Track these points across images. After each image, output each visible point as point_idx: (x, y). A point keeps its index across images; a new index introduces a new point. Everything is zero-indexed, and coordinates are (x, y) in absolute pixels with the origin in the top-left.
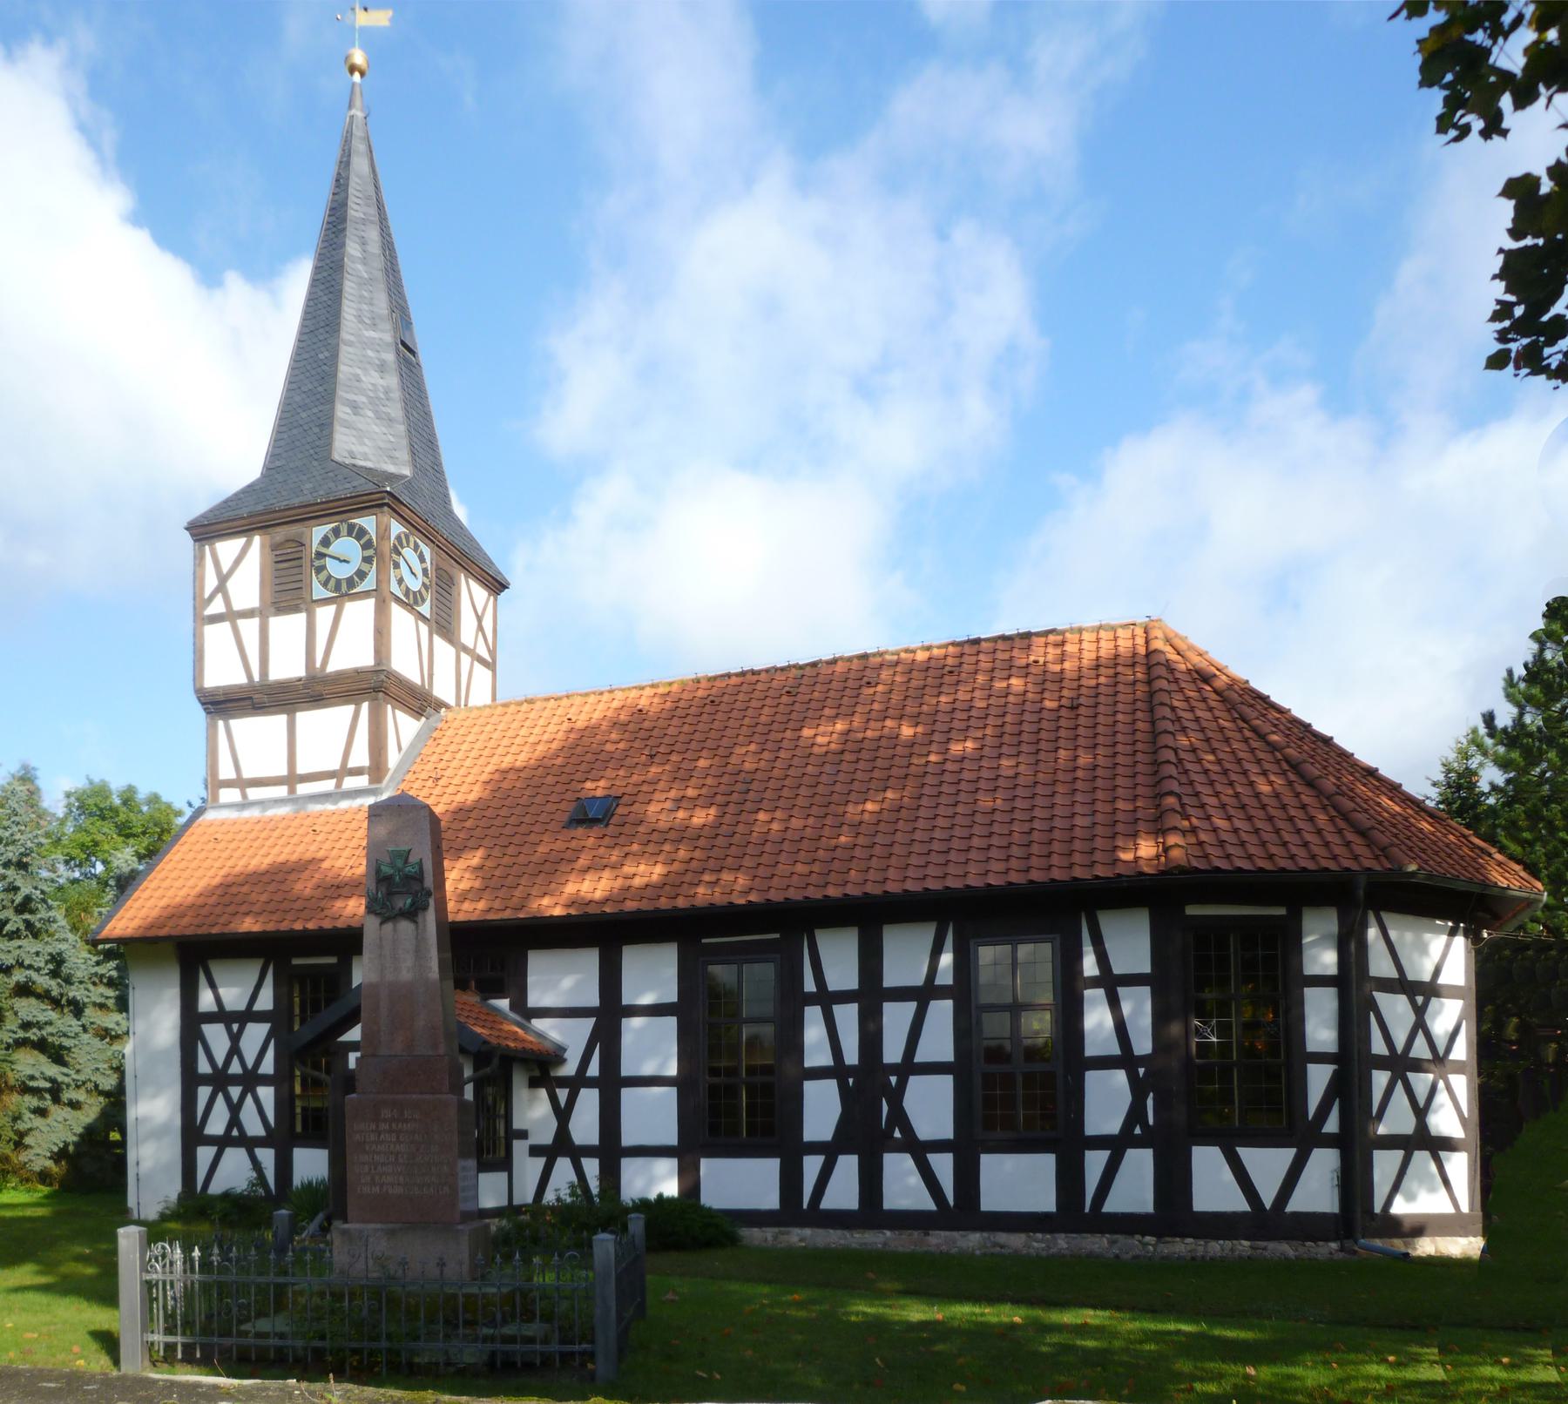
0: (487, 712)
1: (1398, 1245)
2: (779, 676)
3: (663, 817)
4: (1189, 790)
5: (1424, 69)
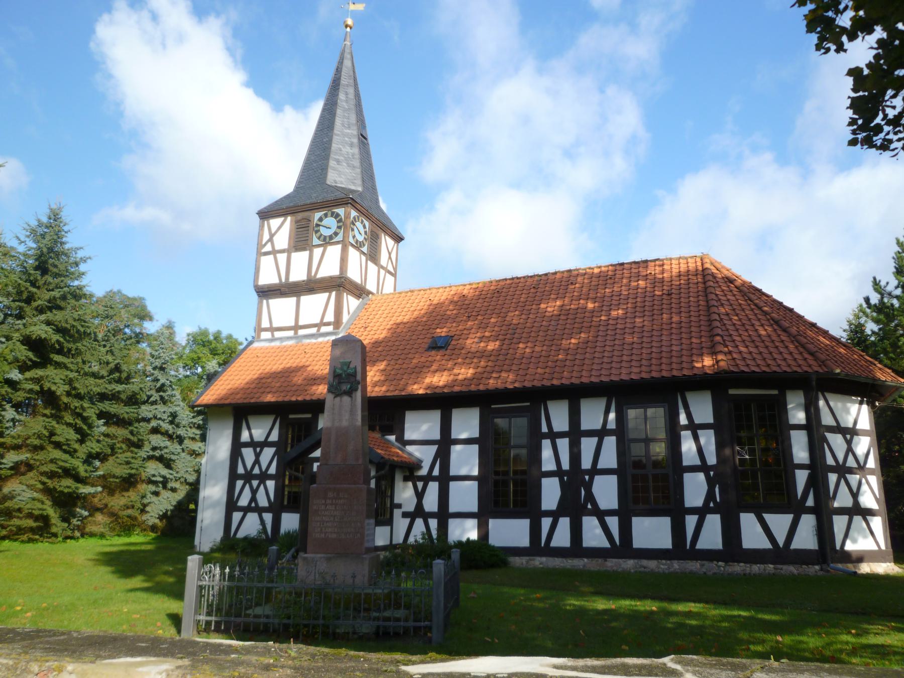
0: (391, 296)
1: (850, 567)
2: (529, 280)
3: (473, 346)
4: (726, 333)
5: (807, 26)
